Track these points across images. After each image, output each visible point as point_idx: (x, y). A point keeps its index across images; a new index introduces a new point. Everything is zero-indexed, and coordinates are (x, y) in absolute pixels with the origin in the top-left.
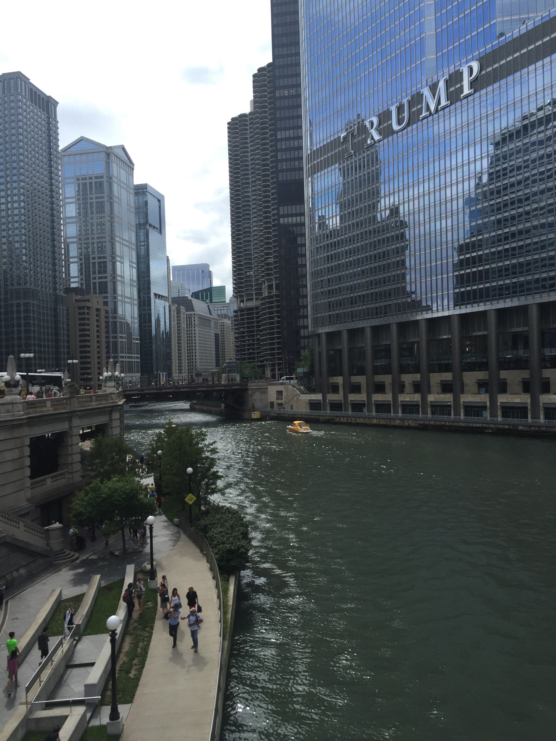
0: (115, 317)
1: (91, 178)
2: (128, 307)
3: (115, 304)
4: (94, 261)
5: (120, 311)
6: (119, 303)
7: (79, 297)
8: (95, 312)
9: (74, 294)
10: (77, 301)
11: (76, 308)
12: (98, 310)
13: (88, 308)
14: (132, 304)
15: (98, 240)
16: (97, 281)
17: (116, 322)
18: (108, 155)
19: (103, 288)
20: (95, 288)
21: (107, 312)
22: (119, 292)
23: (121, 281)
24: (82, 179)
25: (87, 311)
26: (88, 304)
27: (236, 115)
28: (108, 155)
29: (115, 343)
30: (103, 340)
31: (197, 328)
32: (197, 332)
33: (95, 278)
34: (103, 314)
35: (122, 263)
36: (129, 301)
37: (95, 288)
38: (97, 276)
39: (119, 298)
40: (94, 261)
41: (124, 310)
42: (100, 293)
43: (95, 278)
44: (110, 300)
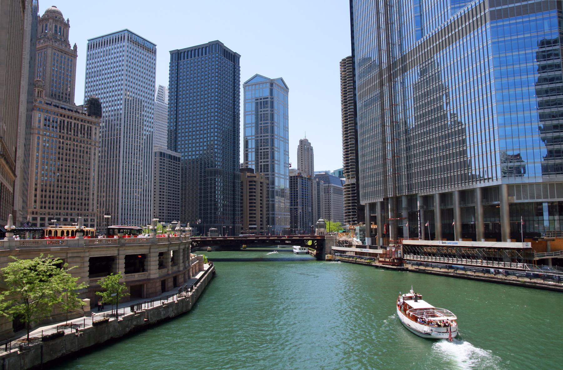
0: (273, 188)
1: (261, 99)
2: (282, 181)
5: (276, 184)
7: (249, 174)
8: (259, 184)
10: (248, 177)
12: (261, 183)
13: (255, 182)
14: (285, 179)
16: (263, 164)
17: (273, 191)
18: (272, 85)
19: (266, 168)
20: (261, 169)
22: (276, 171)
23: (277, 164)
24: (264, 99)
25: (254, 183)
26: (255, 179)
27: (344, 57)
28: (272, 85)
29: (273, 205)
30: (265, 203)
31: (332, 196)
32: (332, 198)
33: (261, 162)
34: (265, 186)
35: (279, 152)
37: (261, 169)
39: (276, 175)
42: (264, 171)
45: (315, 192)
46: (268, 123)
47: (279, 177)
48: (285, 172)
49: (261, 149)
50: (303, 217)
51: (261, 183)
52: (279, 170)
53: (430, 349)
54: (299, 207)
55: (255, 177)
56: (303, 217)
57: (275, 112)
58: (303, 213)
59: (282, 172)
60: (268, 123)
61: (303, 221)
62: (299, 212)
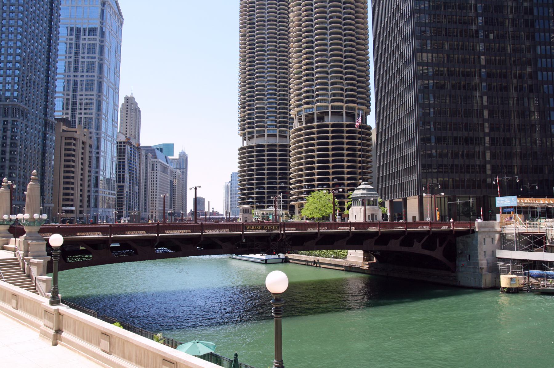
2: (109, 144)
3: (98, 140)
4: (81, 97)
6: (102, 140)
7: (65, 128)
9: (62, 123)
10: (64, 131)
11: (63, 139)
12: (83, 143)
13: (75, 139)
15: (87, 78)
21: (90, 146)
36: (111, 139)
38: (83, 111)
39: (103, 135)
40: (81, 97)
41: (106, 147)
43: (81, 114)
44: (94, 136)
45: (143, 167)
46: (94, 58)
47: (106, 139)
48: (113, 133)
49: (81, 95)
50: (130, 198)
51: (83, 143)
52: (106, 129)
53: (216, 348)
54: (126, 184)
55: (76, 132)
56: (130, 198)
57: (106, 44)
58: (130, 193)
59: (110, 133)
60: (94, 58)
61: (130, 204)
62: (125, 192)
